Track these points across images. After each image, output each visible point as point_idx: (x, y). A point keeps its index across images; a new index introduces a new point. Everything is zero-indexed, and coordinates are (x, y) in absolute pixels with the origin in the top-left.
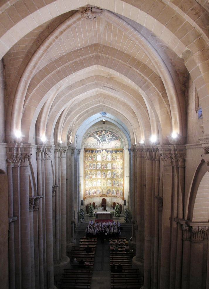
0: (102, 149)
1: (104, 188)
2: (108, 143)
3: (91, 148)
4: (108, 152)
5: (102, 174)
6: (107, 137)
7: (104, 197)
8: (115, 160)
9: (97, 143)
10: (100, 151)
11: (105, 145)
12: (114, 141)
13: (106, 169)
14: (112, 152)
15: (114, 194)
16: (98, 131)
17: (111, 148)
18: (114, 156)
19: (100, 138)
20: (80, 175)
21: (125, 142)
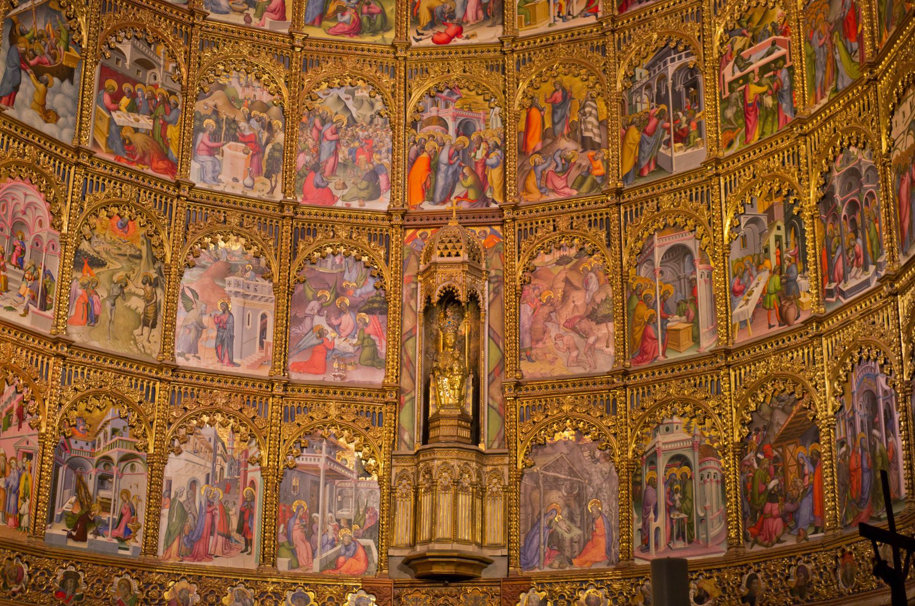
13: (489, 34)
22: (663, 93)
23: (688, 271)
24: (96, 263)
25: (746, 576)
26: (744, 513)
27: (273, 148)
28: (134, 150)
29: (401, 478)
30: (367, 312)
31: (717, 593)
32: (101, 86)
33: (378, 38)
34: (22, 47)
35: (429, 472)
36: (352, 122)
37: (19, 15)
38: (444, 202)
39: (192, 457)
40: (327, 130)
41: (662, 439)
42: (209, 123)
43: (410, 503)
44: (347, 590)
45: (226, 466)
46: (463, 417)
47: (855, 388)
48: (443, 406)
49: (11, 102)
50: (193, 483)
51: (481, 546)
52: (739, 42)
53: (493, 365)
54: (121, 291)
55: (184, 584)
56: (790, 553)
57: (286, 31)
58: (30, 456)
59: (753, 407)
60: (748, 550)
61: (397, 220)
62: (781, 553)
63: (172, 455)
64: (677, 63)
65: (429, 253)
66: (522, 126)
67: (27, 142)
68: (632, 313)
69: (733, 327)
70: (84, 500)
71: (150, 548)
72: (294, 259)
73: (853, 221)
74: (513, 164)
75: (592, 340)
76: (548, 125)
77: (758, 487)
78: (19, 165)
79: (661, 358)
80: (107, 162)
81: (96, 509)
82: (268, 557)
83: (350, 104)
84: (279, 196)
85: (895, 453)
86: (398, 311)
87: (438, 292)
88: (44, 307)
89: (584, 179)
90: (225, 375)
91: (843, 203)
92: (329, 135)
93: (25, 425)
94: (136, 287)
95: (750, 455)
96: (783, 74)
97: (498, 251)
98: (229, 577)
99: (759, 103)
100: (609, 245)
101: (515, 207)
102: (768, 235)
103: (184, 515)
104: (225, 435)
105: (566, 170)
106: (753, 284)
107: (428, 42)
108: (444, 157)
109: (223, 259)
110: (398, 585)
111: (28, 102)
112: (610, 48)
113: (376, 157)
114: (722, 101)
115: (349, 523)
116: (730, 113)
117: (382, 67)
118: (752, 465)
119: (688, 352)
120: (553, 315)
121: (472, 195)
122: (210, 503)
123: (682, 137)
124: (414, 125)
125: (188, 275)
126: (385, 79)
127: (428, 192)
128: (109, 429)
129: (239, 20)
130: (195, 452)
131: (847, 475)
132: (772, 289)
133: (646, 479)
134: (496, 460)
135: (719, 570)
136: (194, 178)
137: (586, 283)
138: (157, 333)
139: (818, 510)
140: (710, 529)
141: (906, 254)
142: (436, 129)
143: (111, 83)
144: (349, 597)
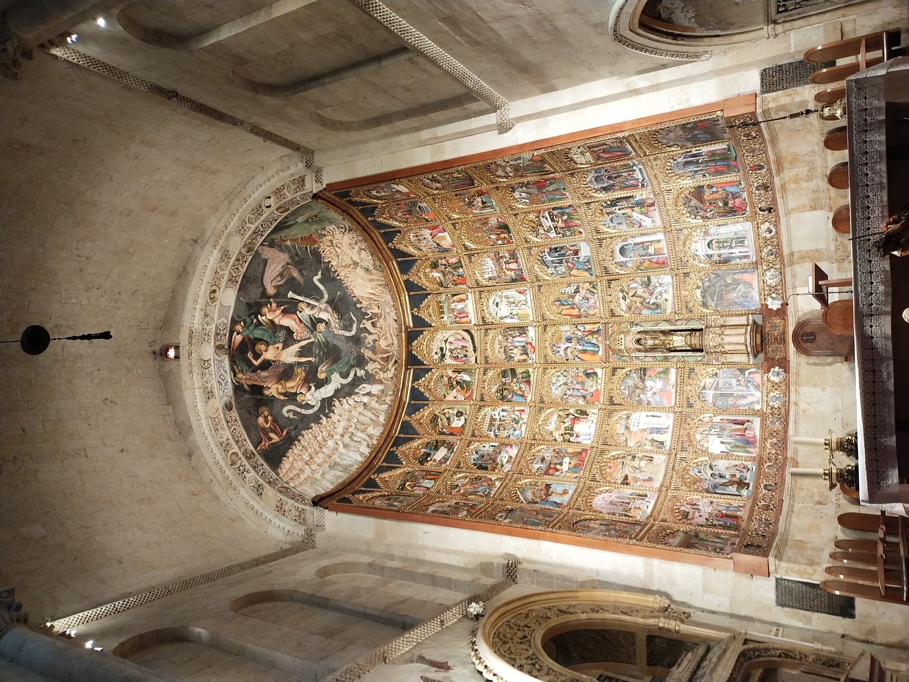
1: (695, 341)
2: (368, 325)
6: (321, 327)
7: (783, 340)
9: (366, 399)
10: (413, 382)
11: (383, 344)
12: (347, 283)
13: (531, 332)
14: (417, 295)
15: (741, 241)
18: (436, 275)
21: (278, 192)
22: (558, 261)
23: (630, 246)
24: (626, 477)
25: (760, 212)
26: (733, 215)
27: (576, 413)
28: (578, 464)
29: (718, 360)
30: (645, 375)
31: (767, 224)
33: (532, 375)
34: (538, 500)
36: (566, 384)
37: (526, 501)
38: (599, 347)
39: (710, 443)
40: (569, 393)
41: (700, 253)
42: (567, 437)
43: (728, 356)
44: (768, 380)
45: (713, 430)
46: (690, 335)
47: (682, 172)
48: (686, 343)
49: (561, 504)
51: (747, 326)
52: (541, 231)
53: (667, 324)
55: (768, 445)
56: (750, 194)
57: (529, 409)
58: (712, 502)
59: (688, 215)
60: (748, 213)
62: (750, 197)
63: (709, 451)
64: (547, 256)
67: (577, 499)
68: (647, 269)
69: (654, 226)
70: (731, 483)
72: (622, 405)
73: (615, 177)
74: (583, 320)
75: (658, 285)
77: (722, 210)
78: (586, 503)
79: (666, 255)
80: (584, 472)
81: (735, 479)
82: (755, 413)
83: (558, 385)
84: (596, 411)
85: (709, 152)
86: (643, 363)
87: (637, 346)
88: (646, 496)
89: (591, 291)
91: (608, 182)
93: (697, 503)
94: (636, 463)
95: (708, 215)
96: (555, 212)
97: (620, 325)
99: (566, 221)
100: (618, 279)
102: (618, 214)
103: (737, 446)
104: (701, 429)
106: (637, 218)
107: (534, 355)
108: (580, 348)
109: (623, 432)
110: (767, 359)
111: (561, 499)
112: (539, 283)
113: (580, 374)
114: (563, 237)
116: (568, 234)
117: (544, 373)
118: (713, 214)
119: (663, 245)
120: (647, 301)
121: (596, 336)
122: (731, 436)
123: (576, 252)
125: (630, 444)
127: (595, 353)
128: (698, 474)
129: (524, 427)
132: (640, 210)
133: (718, 258)
135: (757, 224)
136: (589, 442)
138: (655, 456)
139: (731, 183)
140: (740, 230)
141: (631, 153)
142: (569, 351)
143: (551, 472)
144: (772, 379)
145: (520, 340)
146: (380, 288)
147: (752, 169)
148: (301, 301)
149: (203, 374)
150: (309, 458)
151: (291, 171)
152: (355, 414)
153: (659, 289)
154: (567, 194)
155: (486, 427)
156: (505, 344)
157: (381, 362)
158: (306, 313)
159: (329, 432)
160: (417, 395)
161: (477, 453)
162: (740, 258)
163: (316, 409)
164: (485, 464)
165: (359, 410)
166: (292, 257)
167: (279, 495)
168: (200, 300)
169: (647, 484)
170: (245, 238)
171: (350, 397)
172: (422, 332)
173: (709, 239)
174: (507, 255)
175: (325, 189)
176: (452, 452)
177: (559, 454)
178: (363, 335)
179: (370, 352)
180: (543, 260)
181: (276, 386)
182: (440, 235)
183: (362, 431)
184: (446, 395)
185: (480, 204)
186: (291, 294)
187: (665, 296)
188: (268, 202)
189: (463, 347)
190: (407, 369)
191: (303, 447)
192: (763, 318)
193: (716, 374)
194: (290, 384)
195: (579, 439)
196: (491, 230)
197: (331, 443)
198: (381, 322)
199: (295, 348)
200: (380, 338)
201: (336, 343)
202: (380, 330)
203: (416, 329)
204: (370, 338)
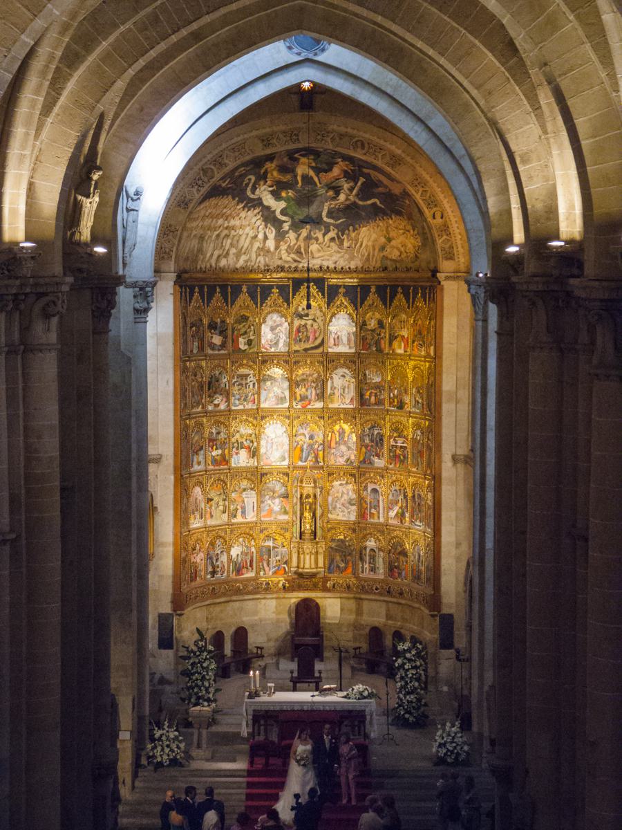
0: (296, 275)
1: (307, 536)
2: (332, 234)
3: (223, 270)
4: (331, 294)
5: (292, 436)
6: (331, 193)
7: (307, 589)
8: (380, 350)
9: (261, 236)
10: (278, 287)
11: (314, 247)
13: (319, 405)
15: (373, 569)
16: (270, 158)
17: (356, 271)
18: (372, 324)
19: (283, 204)
20: (152, 451)
21: (445, 229)
24: (211, 500)
30: (284, 497)
32: (209, 446)
35: (303, 548)
38: (305, 461)
41: (368, 543)
43: (296, 555)
46: (312, 533)
50: (238, 555)
52: (395, 435)
53: (321, 513)
54: (218, 507)
57: (255, 407)
61: (291, 469)
65: (302, 482)
66: (329, 438)
68: (361, 504)
70: (214, 567)
71: (228, 576)
76: (338, 440)
84: (256, 464)
90: (244, 523)
92: (270, 441)
94: (221, 503)
98: (248, 580)
99: (400, 457)
101: (327, 467)
105: (342, 456)
108: (305, 447)
115: (279, 561)
116: (391, 454)
119: (376, 520)
121: (314, 460)
123: (378, 456)
124: (296, 436)
125: (233, 495)
126: (287, 420)
127: (300, 459)
129: (241, 407)
130: (238, 546)
131: (413, 570)
134: (321, 543)
137: (348, 494)
138: (226, 514)
142: (302, 437)
143: (211, 443)
145: (312, 394)
146: (366, 254)
147: (411, 591)
148: (356, 184)
149: (284, 132)
150: (207, 214)
151: (460, 249)
152: (247, 230)
153: (345, 510)
154: (414, 470)
155: (243, 371)
156: (310, 379)
157: (296, 246)
158: (346, 186)
159: (230, 215)
160: (266, 291)
161: (220, 373)
162: (363, 567)
163: (252, 196)
164: (213, 386)
165: (252, 231)
166: (396, 195)
167: (181, 228)
168: (355, 132)
169: (208, 516)
170: (409, 186)
171: (263, 221)
172: (323, 294)
173: (377, 551)
174: (382, 397)
175: (440, 282)
176: (219, 350)
177: (223, 445)
178: (323, 228)
179: (305, 235)
180: (374, 427)
181: (273, 165)
182: (403, 345)
183: (232, 245)
184: (267, 323)
185: (417, 399)
186: (362, 180)
187: (341, 514)
188: (438, 215)
189: (308, 338)
190: (289, 279)
191: (217, 204)
192: (322, 578)
193: (284, 546)
194: (275, 173)
195: (234, 456)
196: (400, 393)
197: (220, 221)
198: (334, 246)
199: (312, 173)
200: (319, 244)
201: (316, 203)
202: (327, 245)
203: (326, 288)
204: (319, 235)
